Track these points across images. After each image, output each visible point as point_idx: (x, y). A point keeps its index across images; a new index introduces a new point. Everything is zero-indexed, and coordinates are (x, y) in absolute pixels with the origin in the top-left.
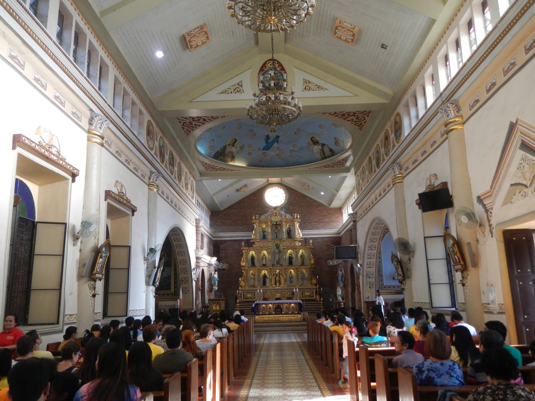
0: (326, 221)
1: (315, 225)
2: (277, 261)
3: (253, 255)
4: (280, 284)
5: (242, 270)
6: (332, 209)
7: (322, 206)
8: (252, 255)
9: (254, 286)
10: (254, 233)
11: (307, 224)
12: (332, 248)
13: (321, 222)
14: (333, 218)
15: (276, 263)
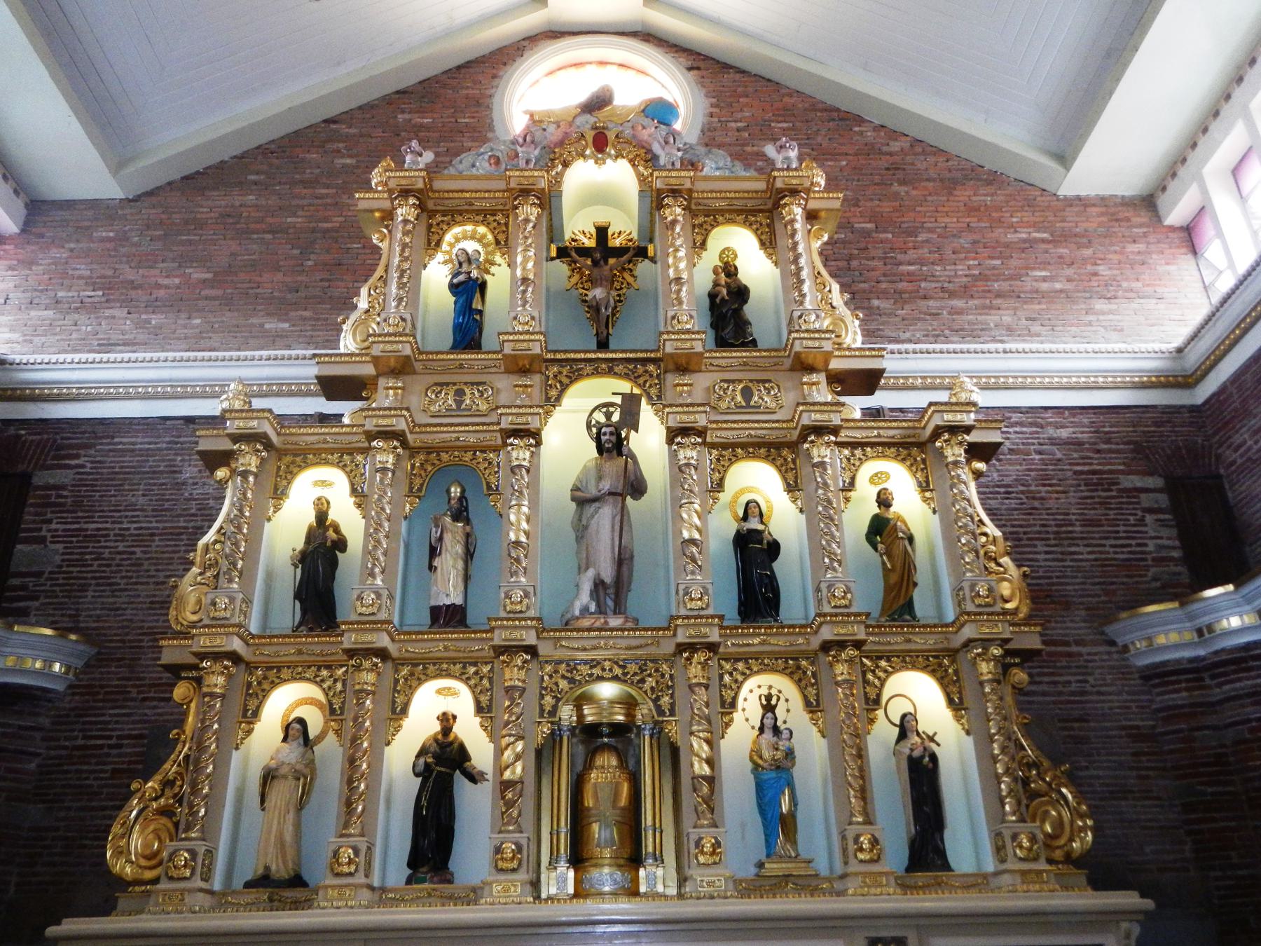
0: (1045, 286)
1: (955, 312)
2: (599, 585)
3: (333, 516)
4: (633, 859)
5: (176, 671)
6: (1081, 203)
7: (989, 183)
8: (322, 517)
9: (297, 881)
10: (363, 304)
11: (876, 303)
12: (1147, 501)
13: (999, 295)
14: (1102, 269)
15: (585, 598)
